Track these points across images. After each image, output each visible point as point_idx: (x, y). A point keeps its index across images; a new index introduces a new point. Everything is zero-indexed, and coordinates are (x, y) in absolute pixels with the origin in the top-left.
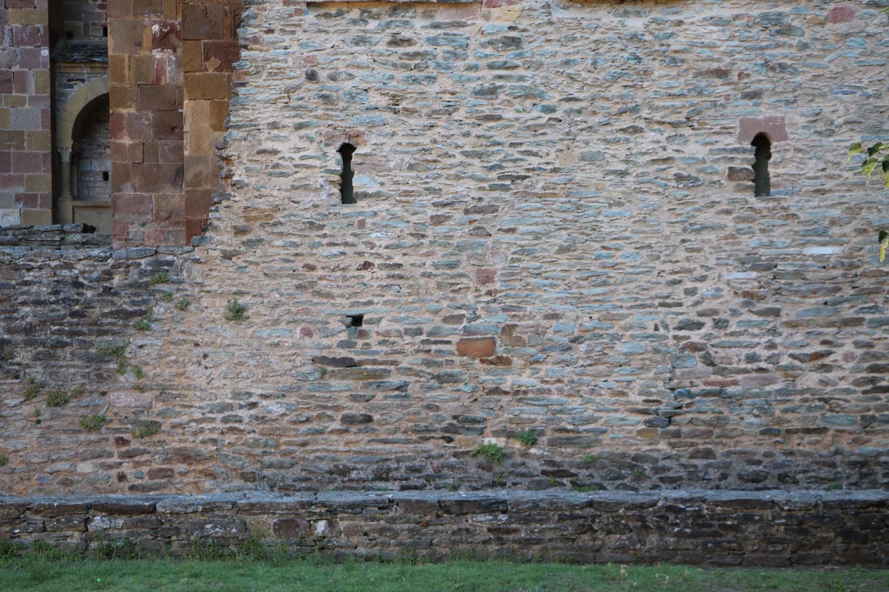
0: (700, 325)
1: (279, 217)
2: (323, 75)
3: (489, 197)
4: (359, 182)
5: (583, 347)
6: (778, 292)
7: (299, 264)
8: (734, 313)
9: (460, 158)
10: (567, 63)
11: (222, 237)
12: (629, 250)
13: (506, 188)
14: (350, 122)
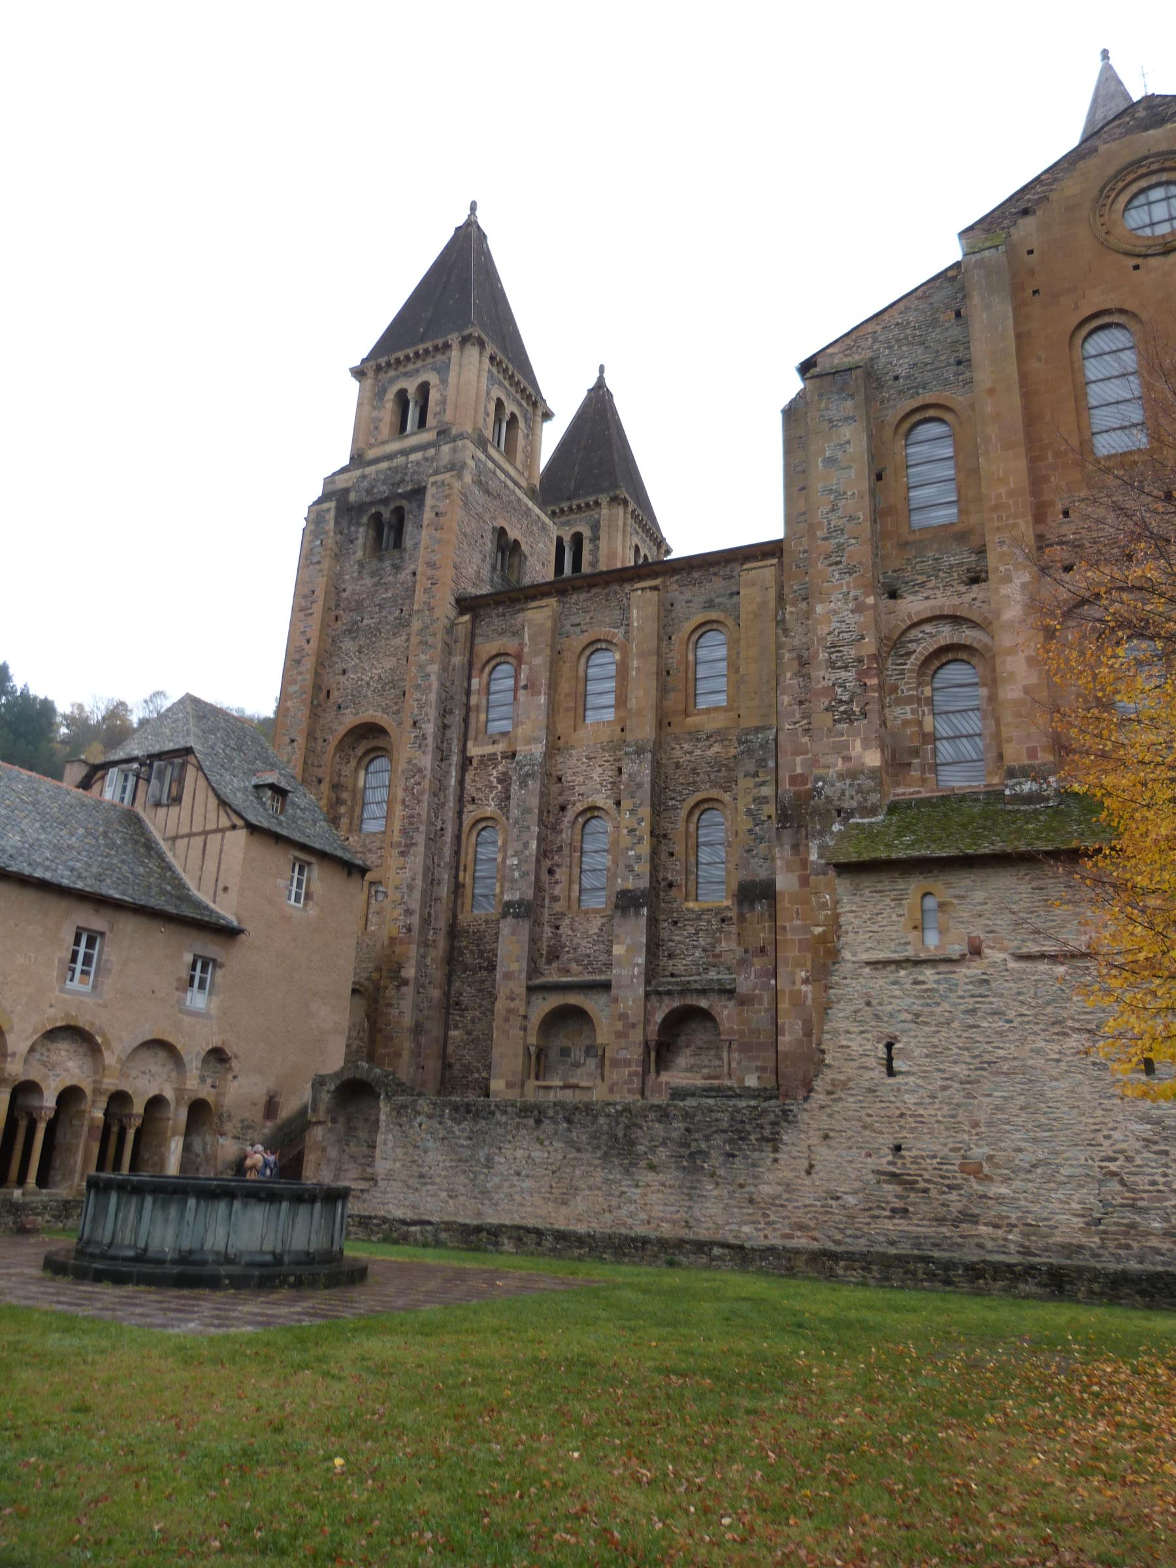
0: (1115, 1159)
1: (851, 1084)
2: (874, 1002)
3: (974, 1075)
4: (897, 1064)
5: (1039, 1171)
6: (1166, 1139)
7: (863, 1113)
8: (1138, 1152)
9: (956, 1050)
10: (1019, 993)
11: (819, 1097)
13: (984, 1069)
14: (891, 1029)
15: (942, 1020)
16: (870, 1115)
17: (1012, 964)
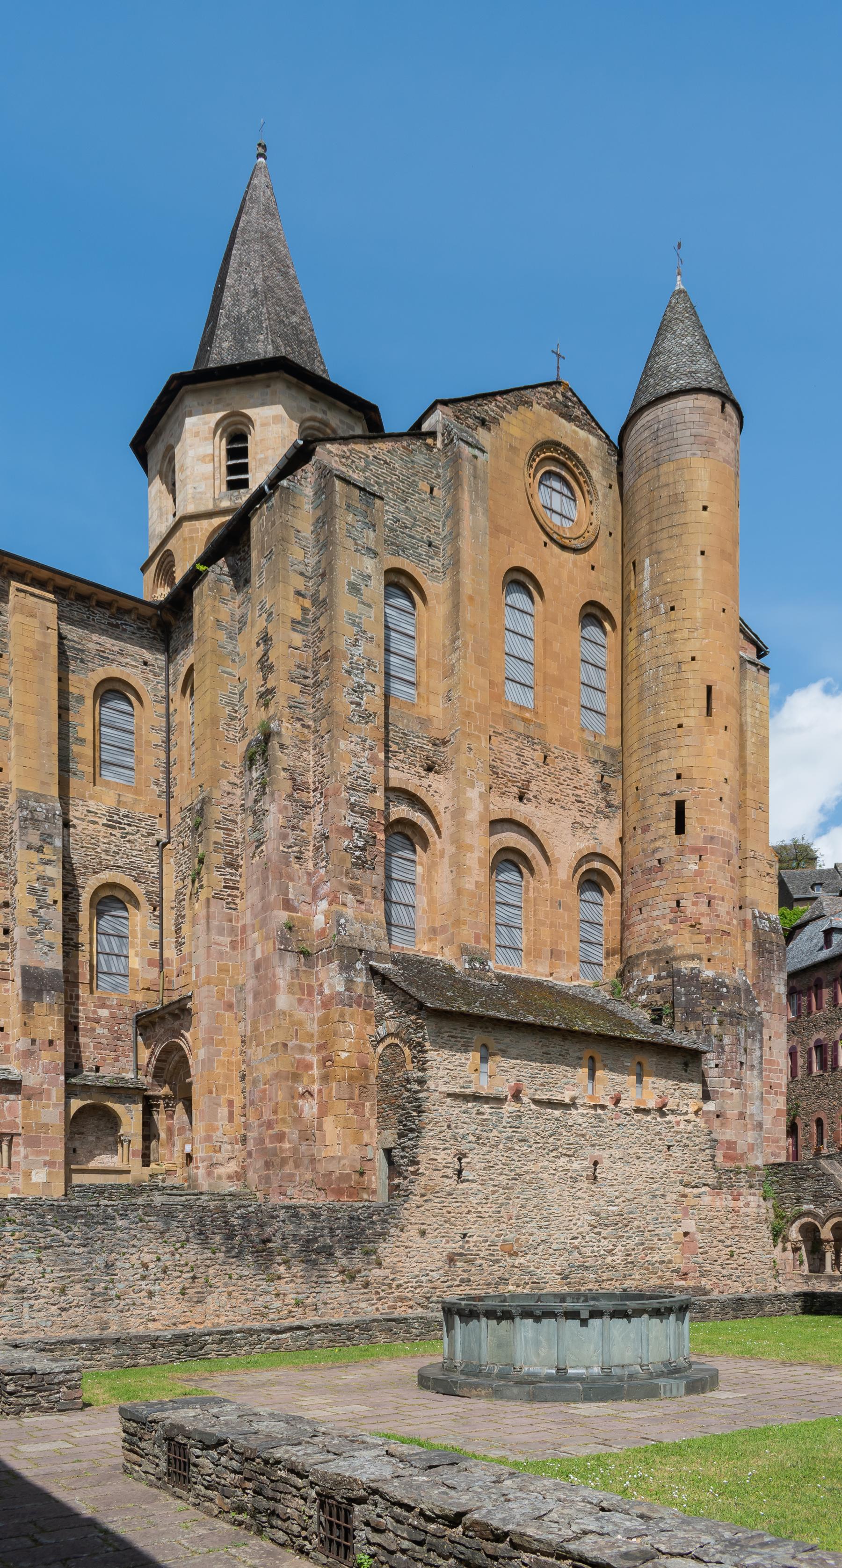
9: (501, 1166)
12: (556, 1207)
15: (493, 1143)
16: (449, 1213)
17: (533, 1107)
